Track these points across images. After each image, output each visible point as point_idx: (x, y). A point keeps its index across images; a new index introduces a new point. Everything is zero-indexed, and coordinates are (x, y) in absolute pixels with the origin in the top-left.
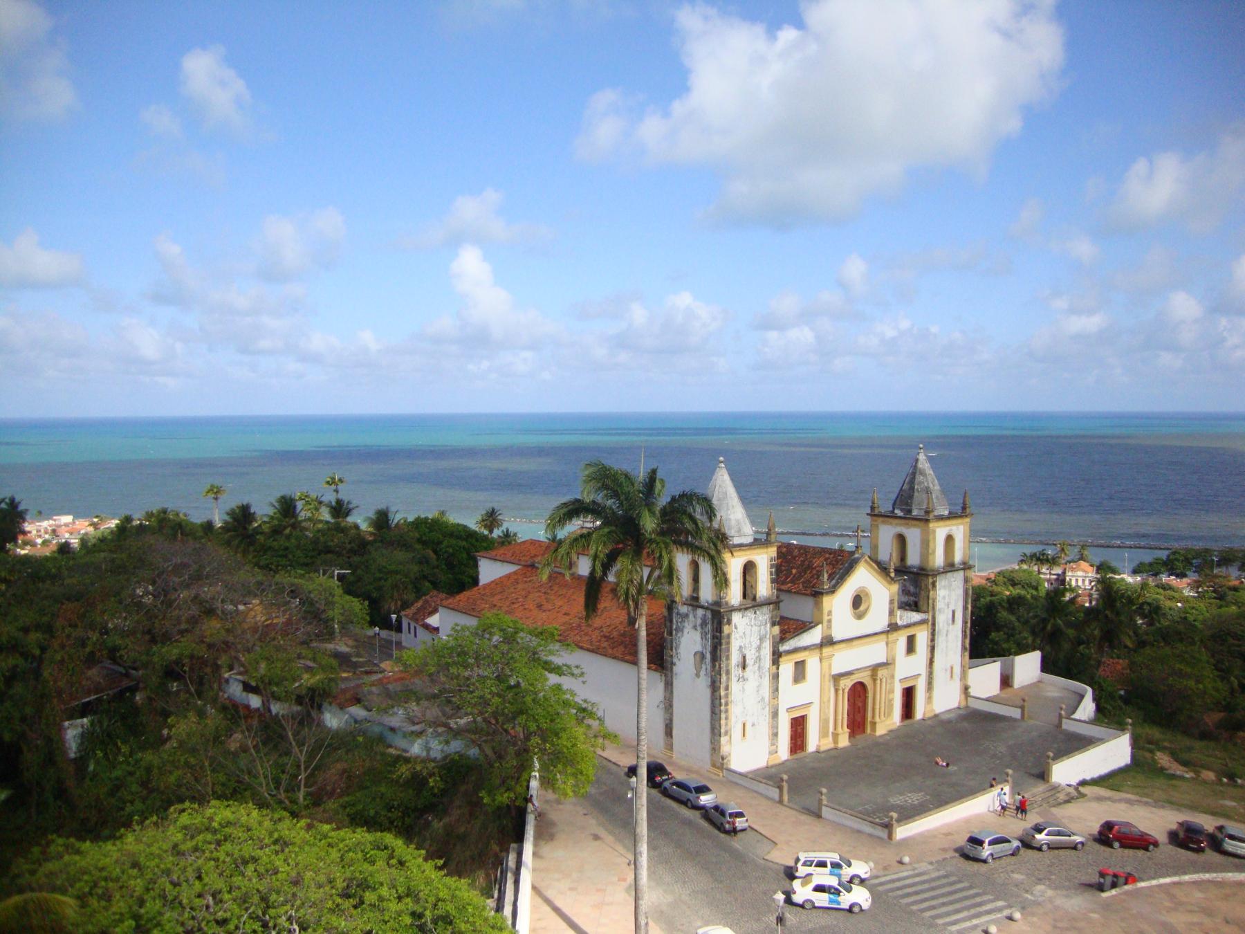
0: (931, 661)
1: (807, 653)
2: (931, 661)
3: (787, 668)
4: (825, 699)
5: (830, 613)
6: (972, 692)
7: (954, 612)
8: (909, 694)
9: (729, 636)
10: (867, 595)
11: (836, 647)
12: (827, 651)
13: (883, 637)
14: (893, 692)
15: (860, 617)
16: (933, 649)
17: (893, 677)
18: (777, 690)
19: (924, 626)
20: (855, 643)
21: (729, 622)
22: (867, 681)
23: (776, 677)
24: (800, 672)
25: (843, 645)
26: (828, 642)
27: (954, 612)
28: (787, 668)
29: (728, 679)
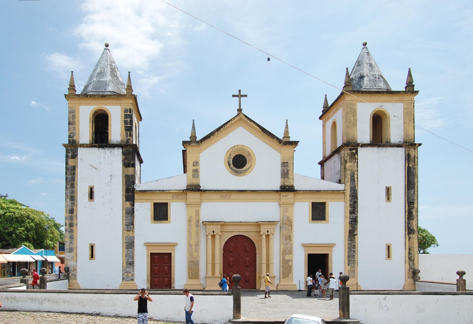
0: (352, 234)
1: (170, 196)
2: (352, 234)
3: (144, 209)
4: (193, 242)
5: (196, 164)
6: (423, 276)
7: (388, 190)
8: (318, 263)
9: (74, 168)
10: (249, 154)
11: (206, 196)
12: (193, 197)
13: (276, 196)
14: (291, 252)
15: (237, 173)
16: (354, 222)
17: (289, 238)
18: (132, 224)
19: (342, 196)
20: (233, 196)
21: (75, 156)
22: (251, 236)
23: (130, 213)
24: (161, 213)
25: (218, 196)
26: (195, 188)
27: (388, 190)
28: (144, 209)
29: (73, 204)
